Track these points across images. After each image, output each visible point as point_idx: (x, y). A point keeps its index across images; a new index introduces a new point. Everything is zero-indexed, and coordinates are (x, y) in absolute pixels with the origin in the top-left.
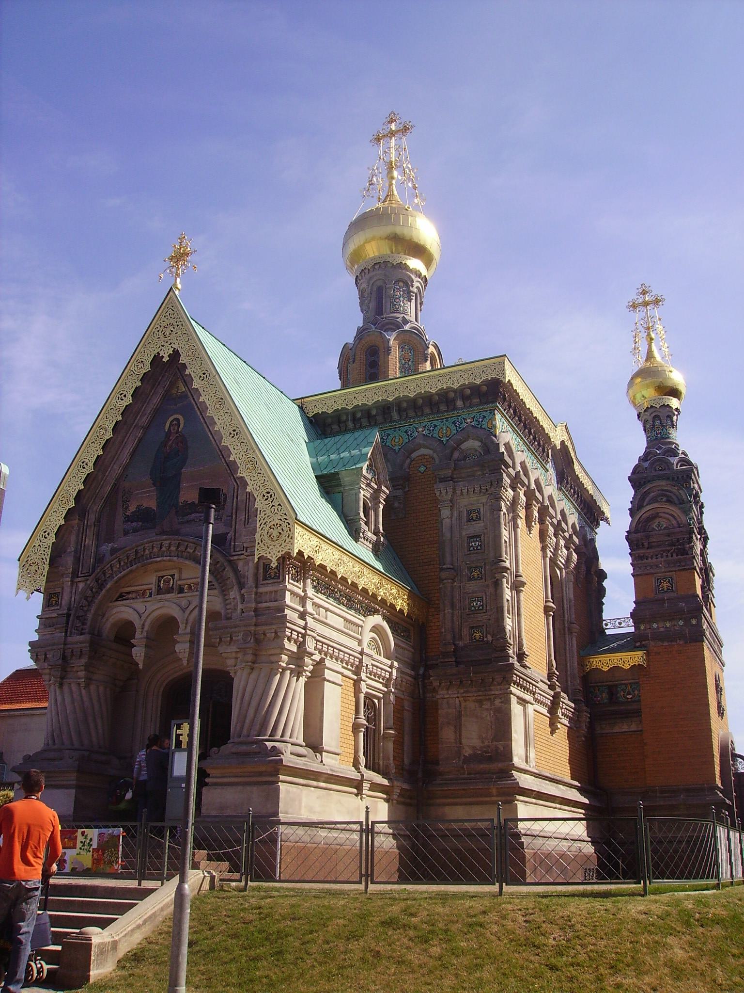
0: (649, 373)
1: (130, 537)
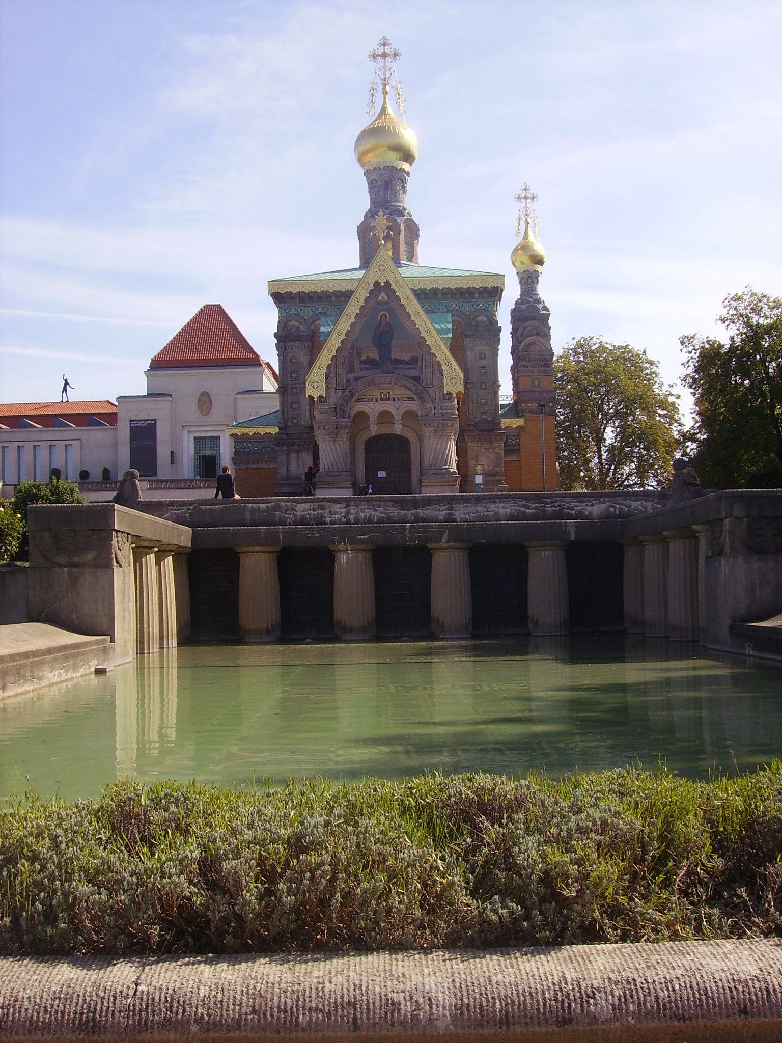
0: (524, 247)
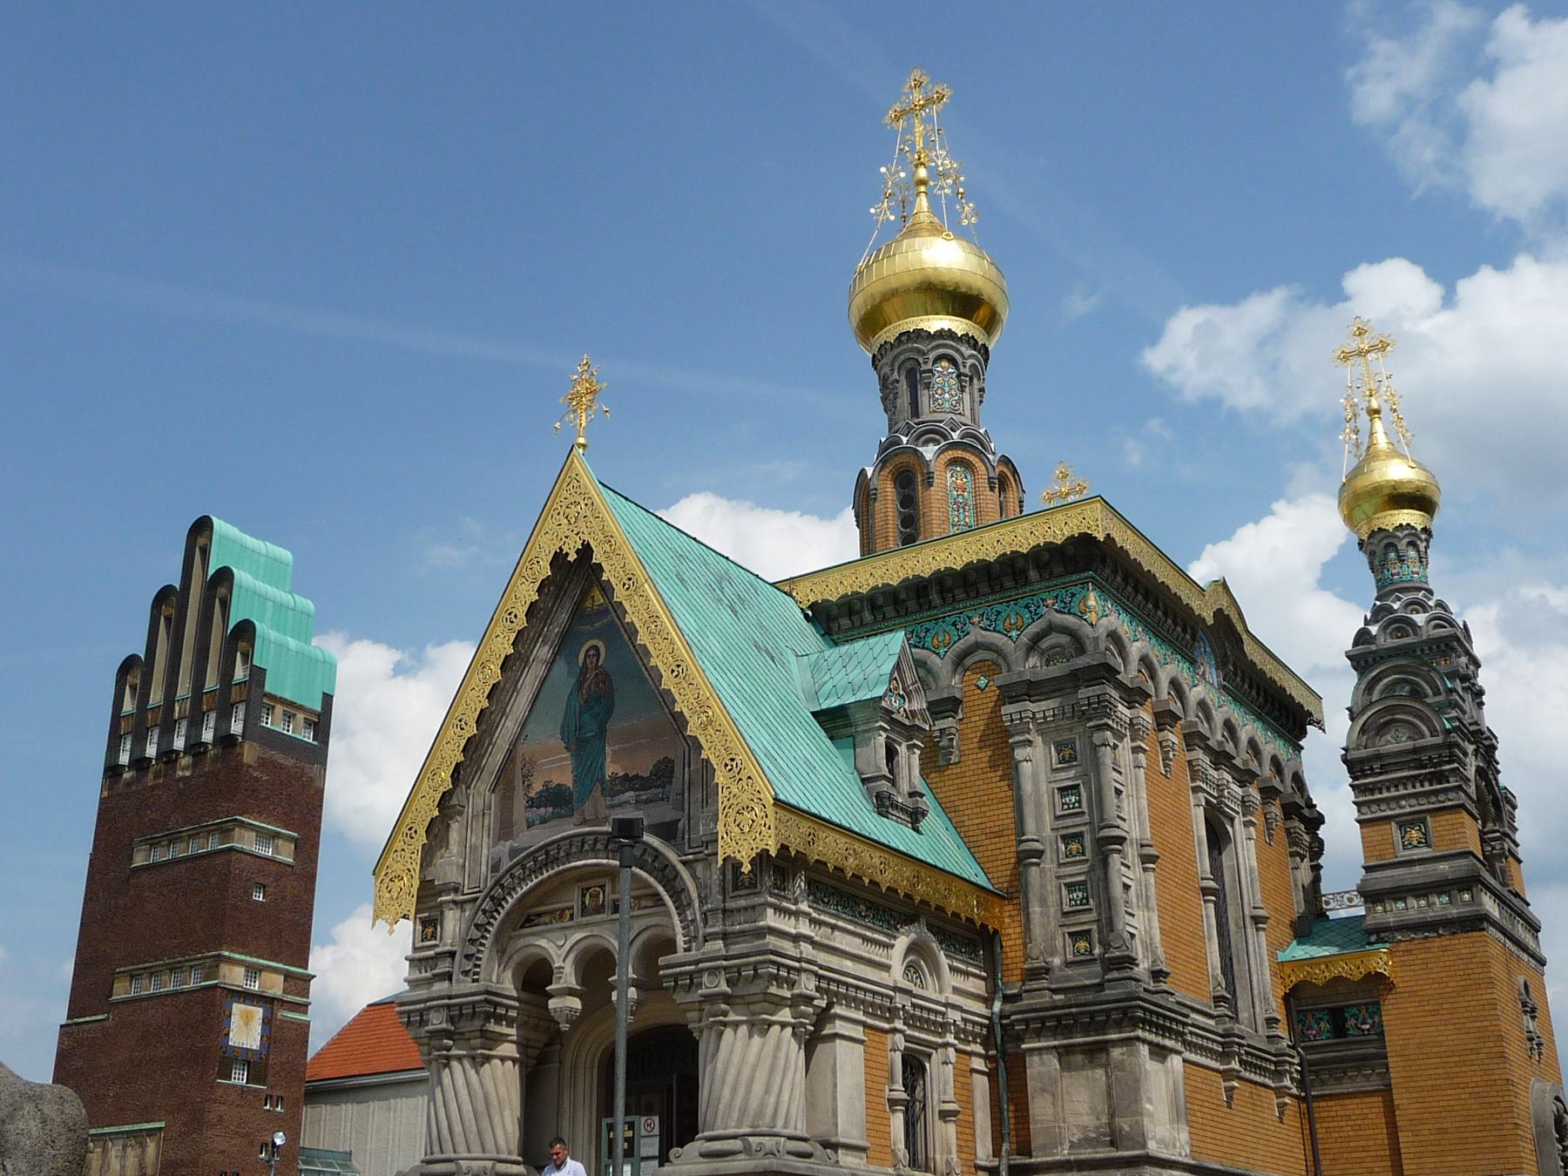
1: (534, 831)
